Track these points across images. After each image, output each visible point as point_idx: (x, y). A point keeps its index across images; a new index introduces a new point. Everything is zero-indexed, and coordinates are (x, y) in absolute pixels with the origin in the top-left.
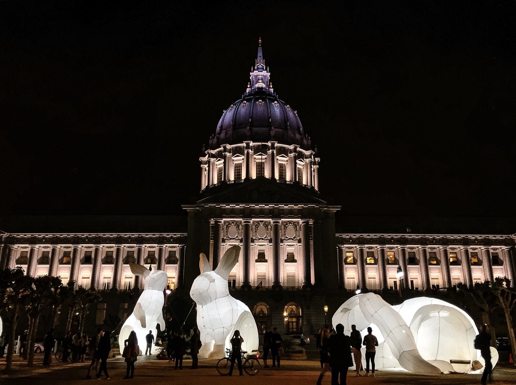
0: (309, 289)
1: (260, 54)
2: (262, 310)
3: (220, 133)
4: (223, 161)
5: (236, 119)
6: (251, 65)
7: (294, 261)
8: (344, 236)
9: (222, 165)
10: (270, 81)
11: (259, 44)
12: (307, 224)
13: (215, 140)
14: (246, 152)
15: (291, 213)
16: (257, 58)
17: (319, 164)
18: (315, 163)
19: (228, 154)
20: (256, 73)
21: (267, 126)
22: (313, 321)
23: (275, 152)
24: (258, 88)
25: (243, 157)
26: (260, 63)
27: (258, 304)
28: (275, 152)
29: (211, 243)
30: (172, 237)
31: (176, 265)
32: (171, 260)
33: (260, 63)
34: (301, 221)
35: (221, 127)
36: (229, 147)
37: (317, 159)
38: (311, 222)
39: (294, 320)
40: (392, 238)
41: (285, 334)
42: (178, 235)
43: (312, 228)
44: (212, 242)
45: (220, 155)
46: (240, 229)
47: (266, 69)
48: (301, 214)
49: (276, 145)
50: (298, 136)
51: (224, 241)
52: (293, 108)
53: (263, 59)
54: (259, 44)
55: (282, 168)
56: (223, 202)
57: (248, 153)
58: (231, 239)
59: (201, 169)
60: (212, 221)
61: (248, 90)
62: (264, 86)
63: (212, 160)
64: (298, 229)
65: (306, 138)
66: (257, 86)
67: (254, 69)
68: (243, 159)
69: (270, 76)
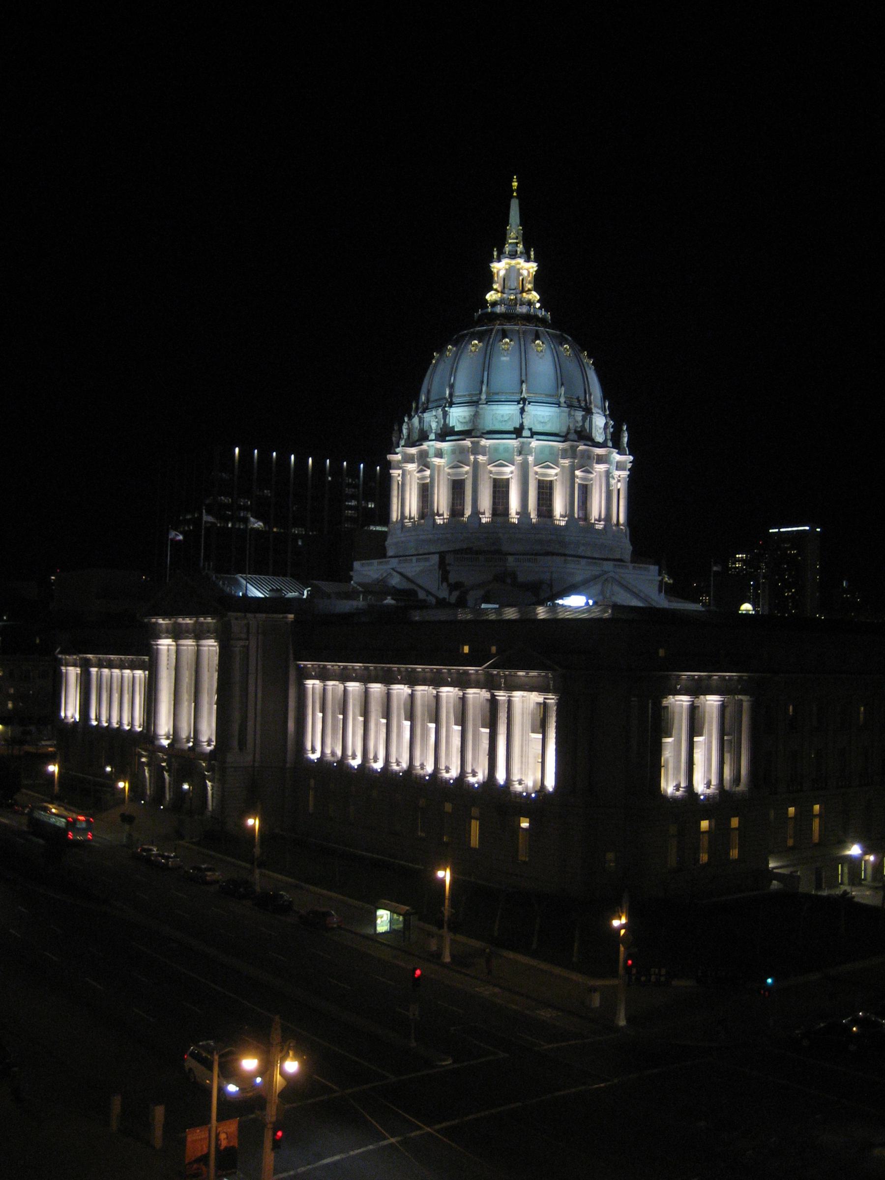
3: (424, 412)
9: (428, 481)
11: (513, 191)
14: (472, 458)
18: (620, 466)
25: (467, 468)
28: (531, 459)
37: (631, 458)
55: (545, 491)
57: (476, 461)
68: (467, 473)
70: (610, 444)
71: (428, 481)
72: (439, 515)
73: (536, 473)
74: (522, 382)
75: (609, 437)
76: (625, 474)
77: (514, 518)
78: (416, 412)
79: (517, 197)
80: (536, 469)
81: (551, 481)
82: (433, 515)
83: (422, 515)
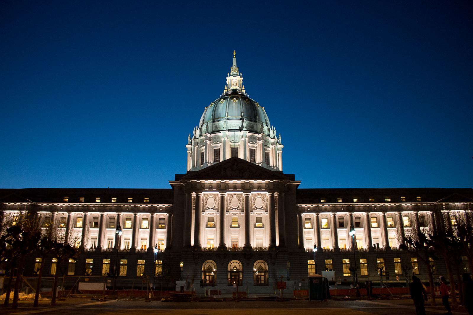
0: (274, 249)
1: (234, 63)
2: (235, 267)
3: (202, 126)
4: (204, 147)
5: (215, 115)
6: (227, 71)
8: (304, 205)
9: (204, 151)
10: (243, 84)
11: (234, 55)
12: (272, 196)
13: (198, 132)
15: (259, 188)
16: (232, 66)
17: (283, 149)
19: (208, 142)
20: (231, 77)
21: (241, 119)
22: (277, 274)
23: (247, 140)
24: (233, 90)
25: (220, 144)
26: (234, 69)
27: (232, 262)
28: (247, 140)
29: (193, 212)
30: (161, 207)
31: (165, 230)
33: (234, 69)
34: (267, 194)
35: (204, 120)
37: (282, 146)
38: (276, 194)
39: (263, 274)
40: (342, 207)
41: (254, 285)
42: (166, 205)
43: (277, 200)
44: (193, 211)
46: (217, 200)
47: (239, 75)
48: (268, 188)
49: (248, 134)
51: (203, 211)
53: (237, 67)
54: (234, 55)
55: (253, 153)
56: (203, 178)
58: (209, 209)
60: (194, 194)
61: (225, 91)
62: (238, 88)
64: (265, 200)
65: (272, 129)
66: (232, 88)
67: (230, 75)
68: (220, 146)
69: (242, 80)
70: (276, 137)
71: (204, 151)
72: (209, 163)
73: (249, 146)
74: (242, 112)
75: (275, 135)
76: (280, 152)
78: (198, 128)
79: (235, 57)
80: (249, 144)
81: (255, 149)
82: (206, 162)
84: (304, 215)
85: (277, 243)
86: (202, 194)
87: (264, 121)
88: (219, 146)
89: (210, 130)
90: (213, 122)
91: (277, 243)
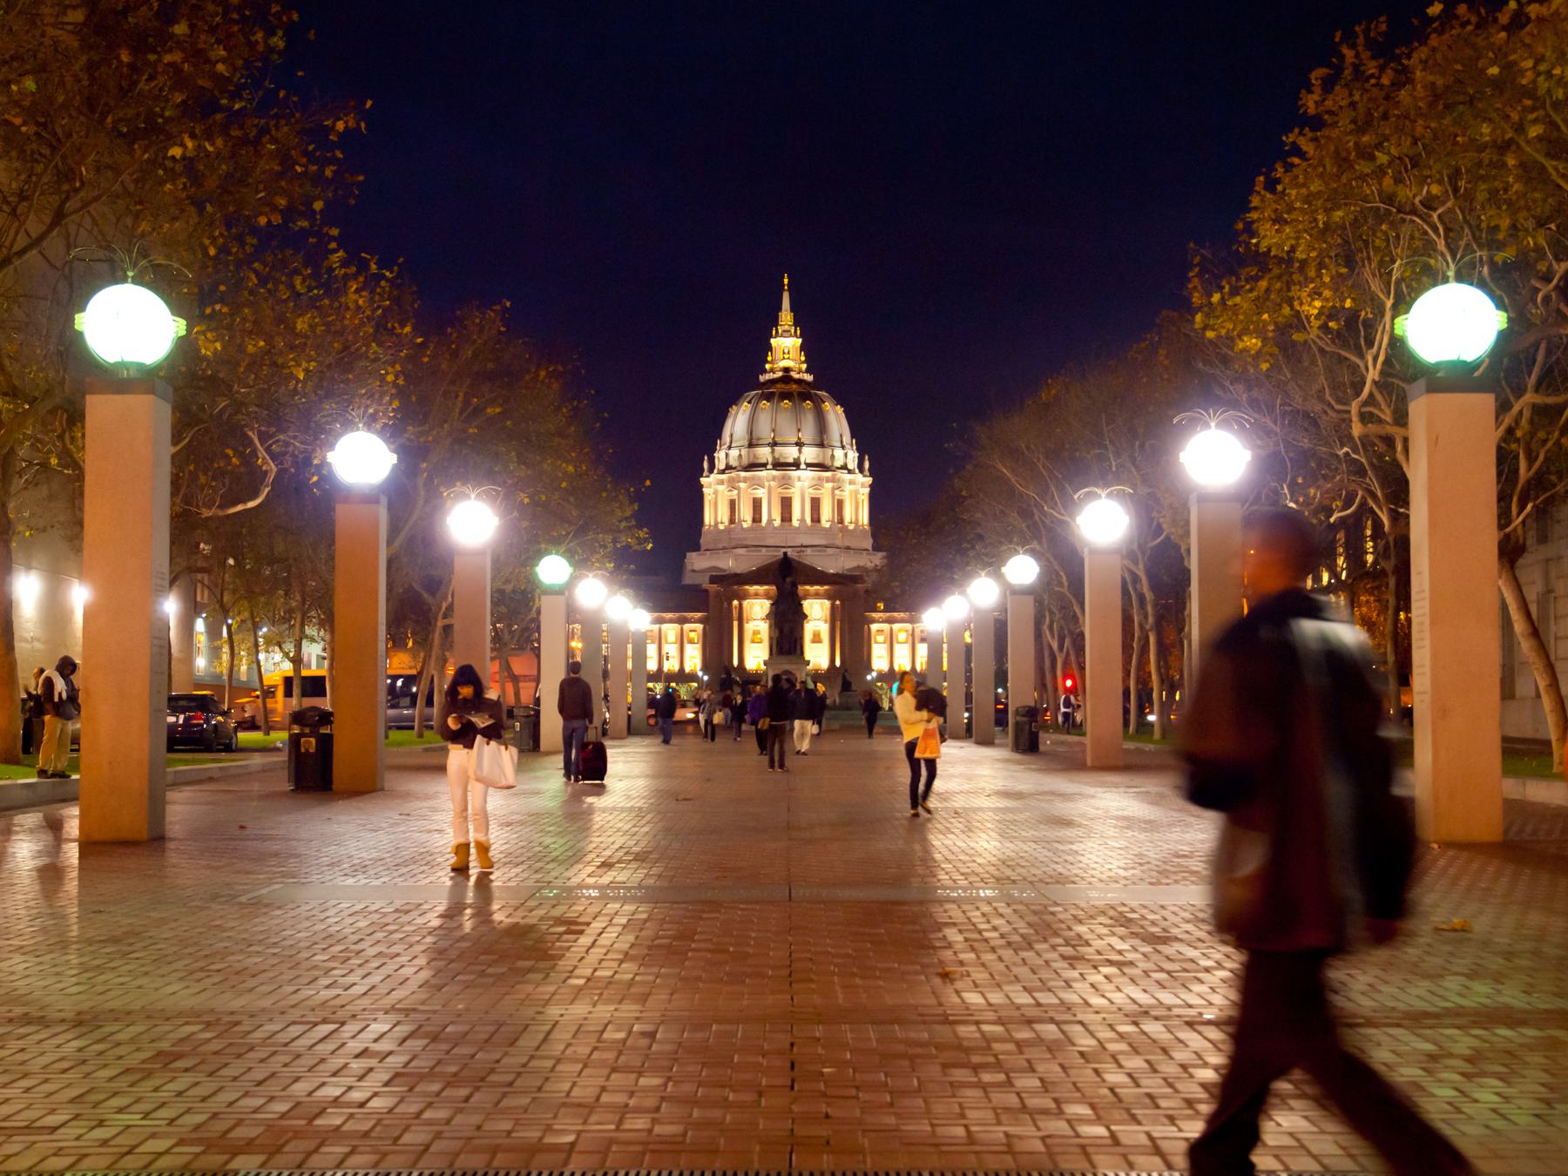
6: (771, 322)
7: (820, 641)
10: (802, 348)
16: (780, 309)
26: (786, 317)
32: (691, 642)
33: (786, 317)
34: (827, 603)
36: (743, 474)
44: (736, 623)
45: (732, 485)
48: (828, 596)
50: (839, 453)
52: (839, 400)
55: (816, 504)
59: (701, 497)
60: (735, 602)
61: (768, 366)
63: (721, 488)
77: (795, 523)
83: (732, 521)
84: (874, 627)
85: (838, 663)
86: (746, 603)
87: (837, 437)
88: (761, 493)
89: (745, 462)
90: (751, 445)
91: (838, 663)
